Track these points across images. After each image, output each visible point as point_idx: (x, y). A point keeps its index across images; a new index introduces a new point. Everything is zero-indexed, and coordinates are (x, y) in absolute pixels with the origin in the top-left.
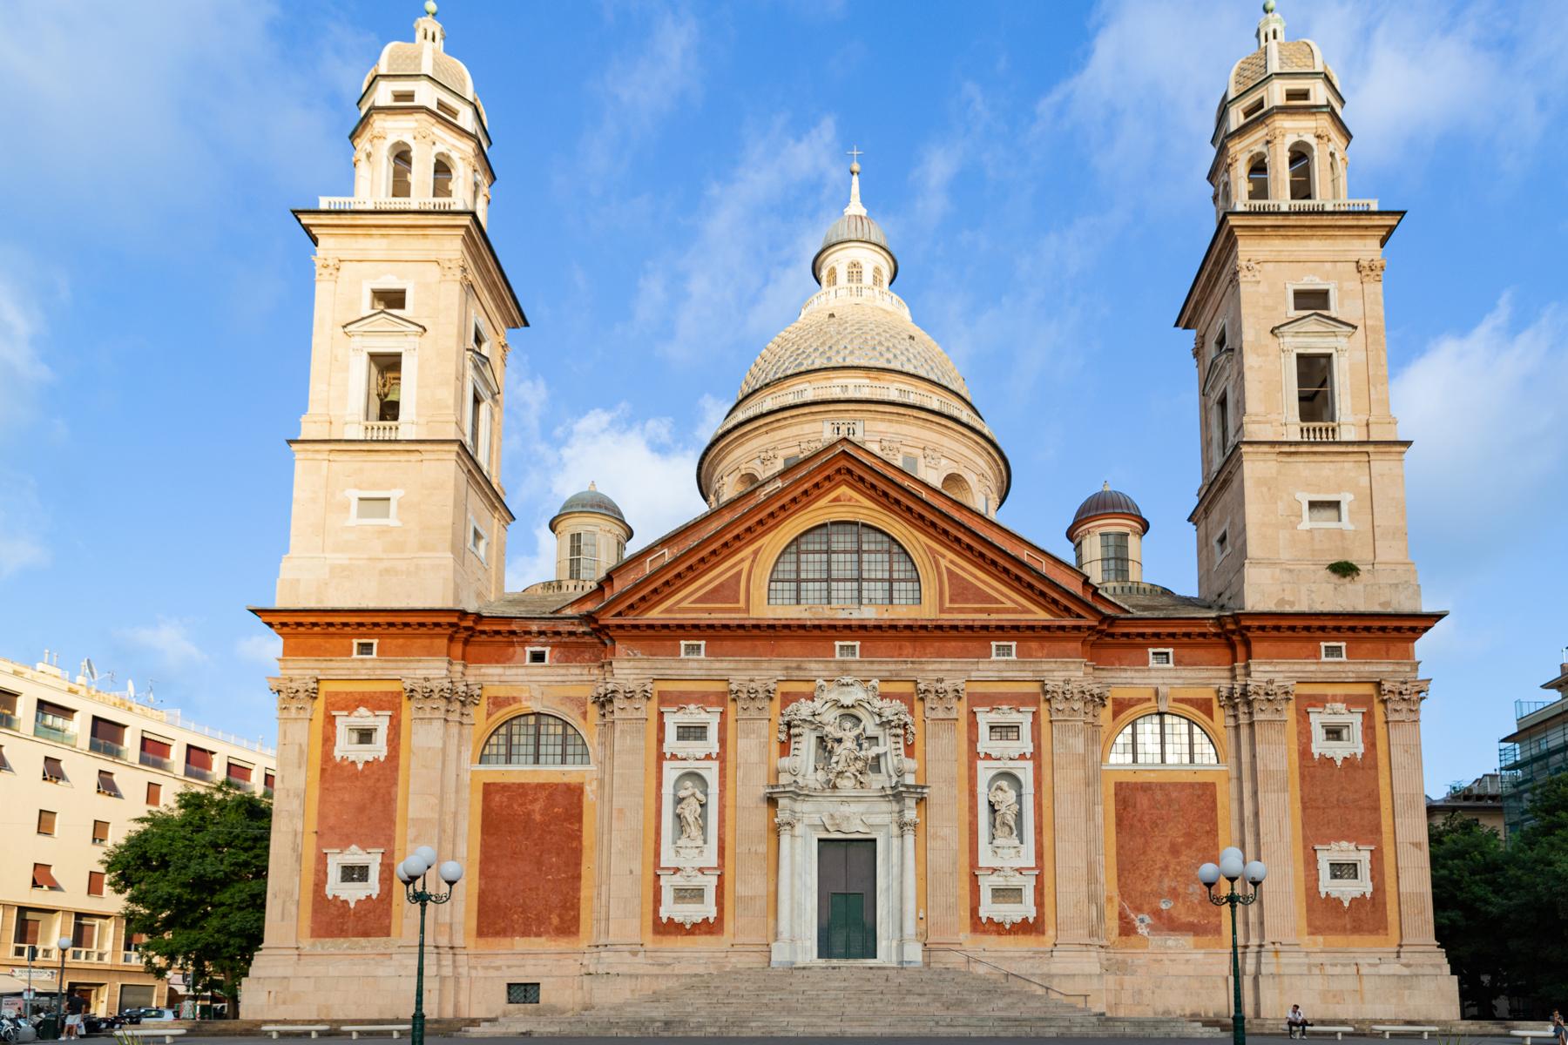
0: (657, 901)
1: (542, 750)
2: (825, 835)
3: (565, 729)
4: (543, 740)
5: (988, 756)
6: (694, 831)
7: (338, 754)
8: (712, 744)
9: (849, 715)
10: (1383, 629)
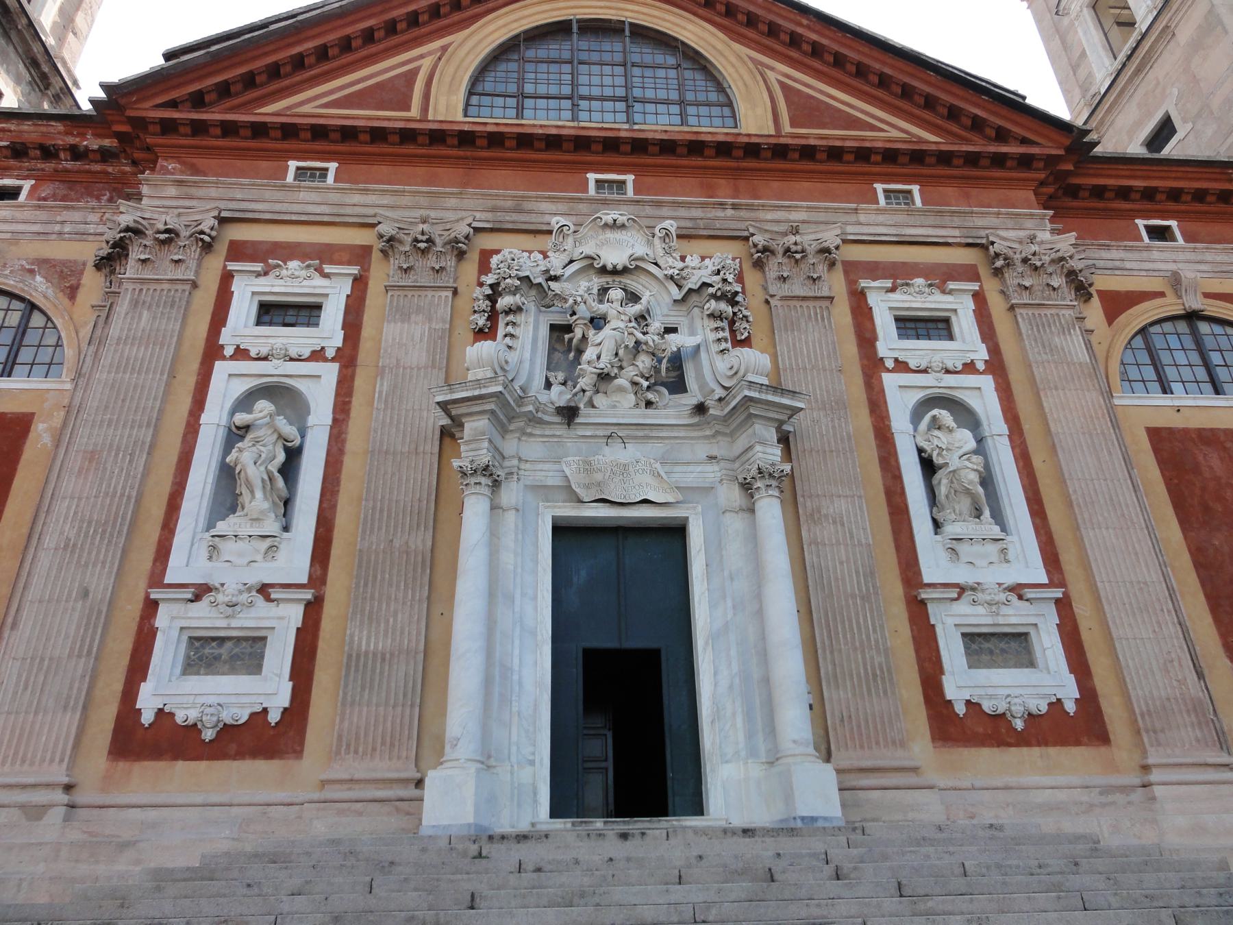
0: (138, 668)
2: (569, 511)
3: (26, 318)
5: (901, 366)
6: (258, 502)
8: (330, 329)
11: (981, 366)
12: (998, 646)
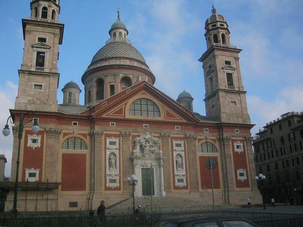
1: (76, 146)
4: (76, 143)
5: (175, 151)
7: (28, 145)
8: (117, 146)
9: (147, 141)
10: (230, 126)
12: (181, 181)
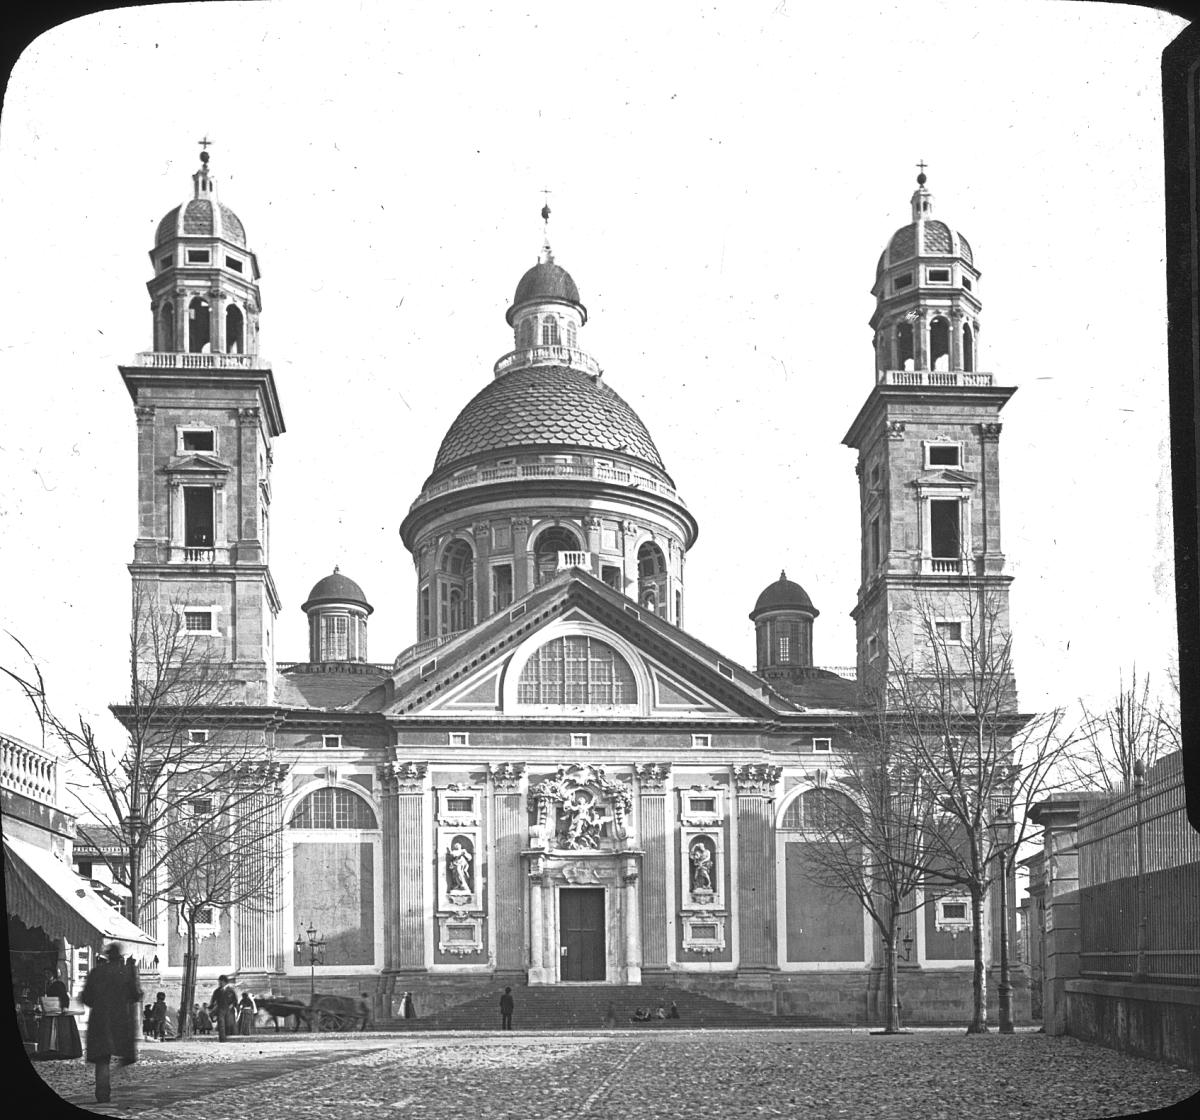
11: (720, 823)
